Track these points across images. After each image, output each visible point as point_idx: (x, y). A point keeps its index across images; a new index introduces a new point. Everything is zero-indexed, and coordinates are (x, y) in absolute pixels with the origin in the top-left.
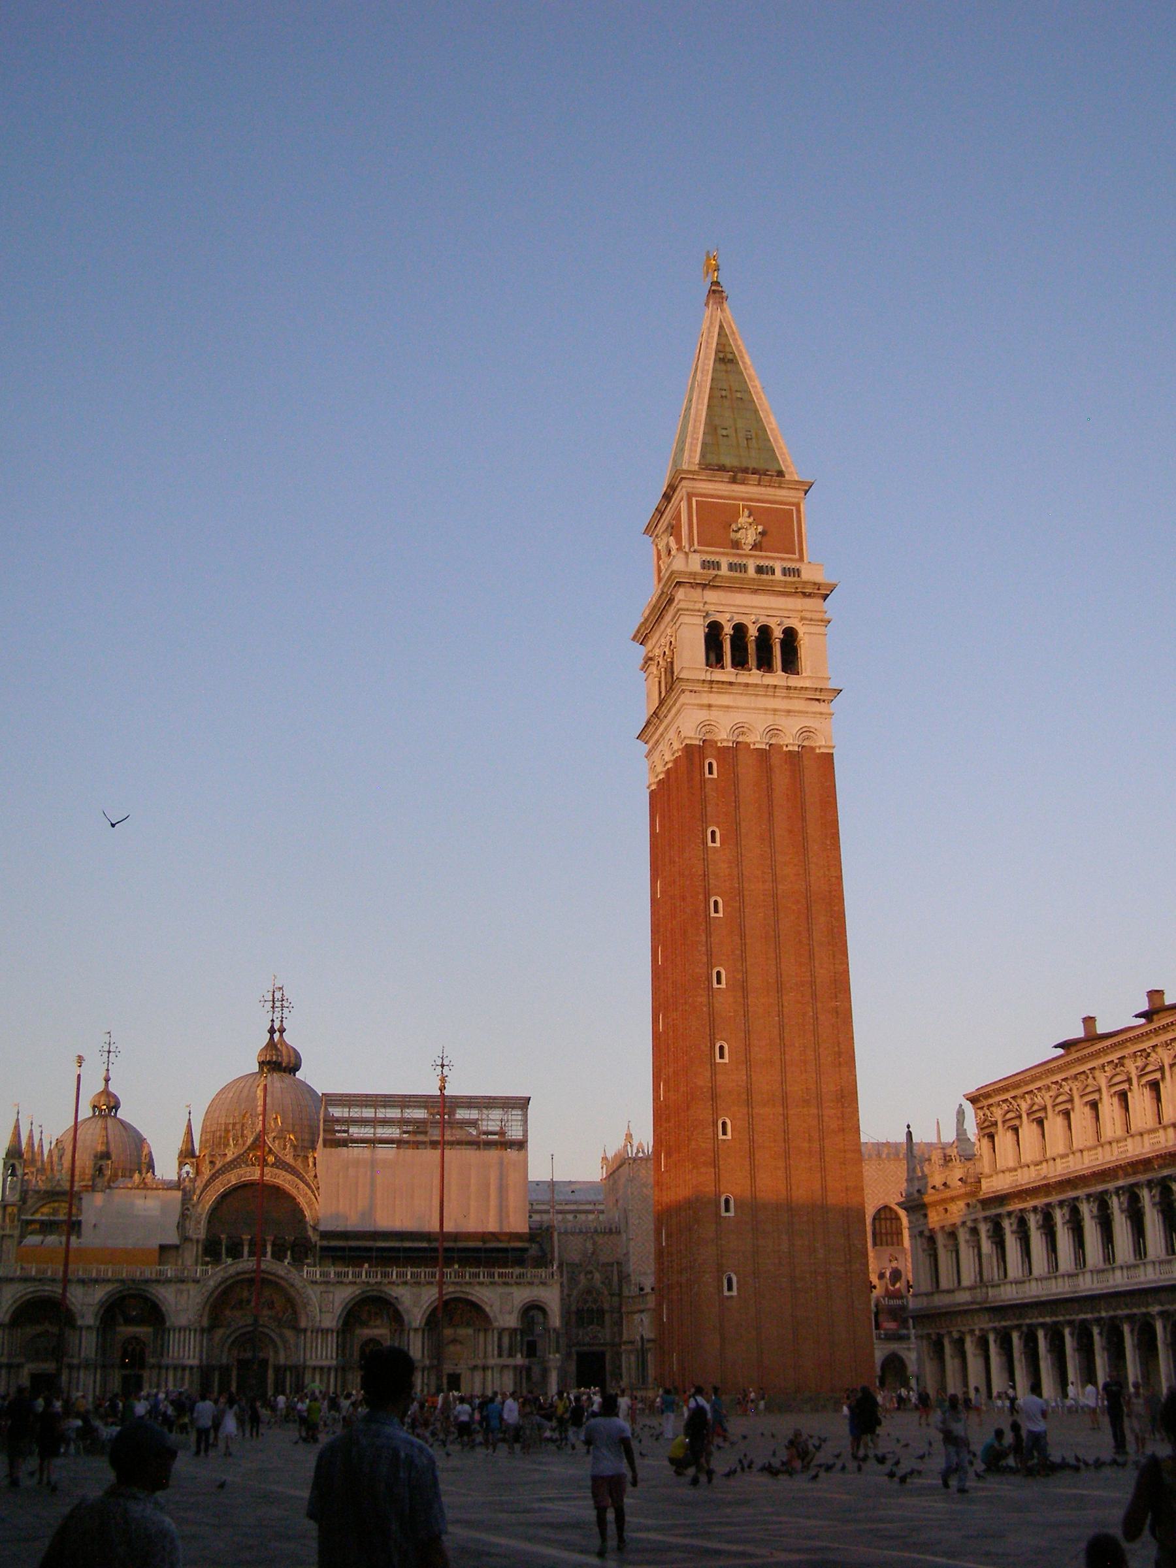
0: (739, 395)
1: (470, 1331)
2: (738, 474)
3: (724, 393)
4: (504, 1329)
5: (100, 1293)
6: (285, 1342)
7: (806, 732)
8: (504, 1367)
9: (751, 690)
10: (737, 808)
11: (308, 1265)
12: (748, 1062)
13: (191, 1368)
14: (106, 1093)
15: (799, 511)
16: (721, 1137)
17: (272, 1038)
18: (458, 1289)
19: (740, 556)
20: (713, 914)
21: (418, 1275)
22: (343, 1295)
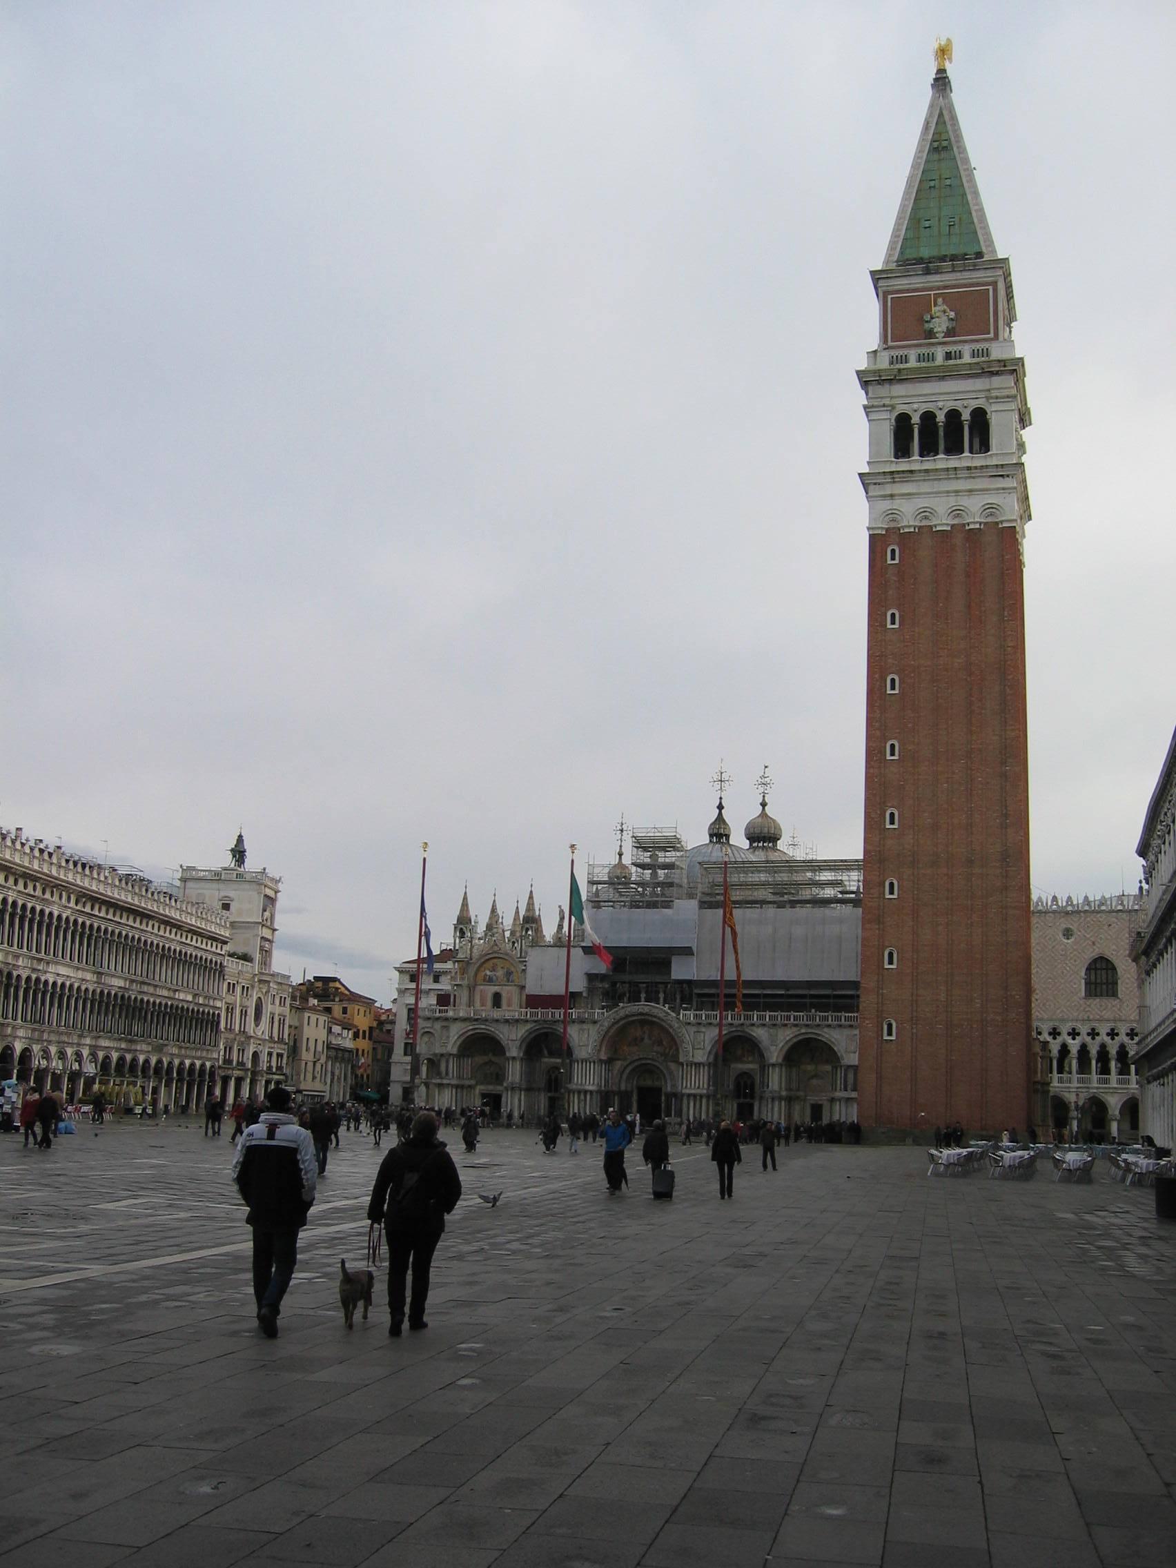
0: (948, 182)
1: (828, 1068)
2: (928, 266)
3: (932, 184)
4: (849, 1067)
5: (521, 1031)
6: (671, 1073)
7: (990, 509)
8: (848, 1100)
11: (685, 1009)
13: (591, 1092)
15: (995, 290)
17: (720, 814)
19: (933, 344)
21: (776, 1018)
22: (710, 1036)
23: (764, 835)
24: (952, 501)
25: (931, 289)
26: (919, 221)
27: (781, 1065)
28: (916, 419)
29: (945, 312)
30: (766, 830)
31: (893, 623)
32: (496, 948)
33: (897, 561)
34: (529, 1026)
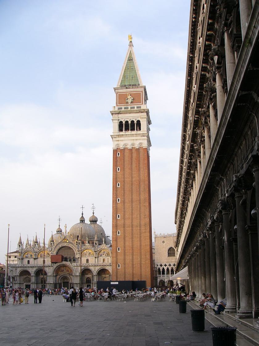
0: (132, 68)
3: (128, 68)
5: (35, 269)
6: (71, 278)
7: (141, 144)
9: (128, 136)
10: (124, 162)
11: (74, 263)
12: (124, 219)
13: (52, 283)
14: (59, 228)
15: (142, 93)
16: (118, 235)
17: (82, 216)
18: (103, 267)
20: (118, 187)
23: (94, 221)
24: (132, 142)
25: (128, 92)
26: (125, 77)
27: (97, 275)
28: (124, 123)
29: (131, 98)
30: (93, 219)
31: (119, 170)
32: (28, 249)
33: (119, 156)
34: (36, 268)
